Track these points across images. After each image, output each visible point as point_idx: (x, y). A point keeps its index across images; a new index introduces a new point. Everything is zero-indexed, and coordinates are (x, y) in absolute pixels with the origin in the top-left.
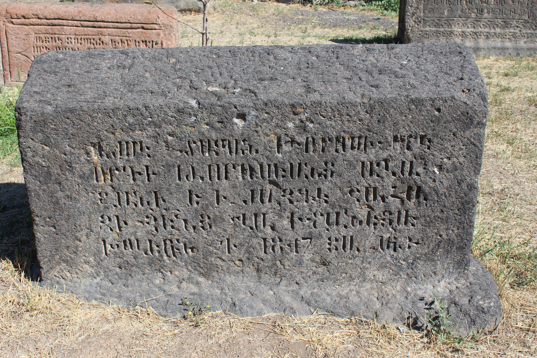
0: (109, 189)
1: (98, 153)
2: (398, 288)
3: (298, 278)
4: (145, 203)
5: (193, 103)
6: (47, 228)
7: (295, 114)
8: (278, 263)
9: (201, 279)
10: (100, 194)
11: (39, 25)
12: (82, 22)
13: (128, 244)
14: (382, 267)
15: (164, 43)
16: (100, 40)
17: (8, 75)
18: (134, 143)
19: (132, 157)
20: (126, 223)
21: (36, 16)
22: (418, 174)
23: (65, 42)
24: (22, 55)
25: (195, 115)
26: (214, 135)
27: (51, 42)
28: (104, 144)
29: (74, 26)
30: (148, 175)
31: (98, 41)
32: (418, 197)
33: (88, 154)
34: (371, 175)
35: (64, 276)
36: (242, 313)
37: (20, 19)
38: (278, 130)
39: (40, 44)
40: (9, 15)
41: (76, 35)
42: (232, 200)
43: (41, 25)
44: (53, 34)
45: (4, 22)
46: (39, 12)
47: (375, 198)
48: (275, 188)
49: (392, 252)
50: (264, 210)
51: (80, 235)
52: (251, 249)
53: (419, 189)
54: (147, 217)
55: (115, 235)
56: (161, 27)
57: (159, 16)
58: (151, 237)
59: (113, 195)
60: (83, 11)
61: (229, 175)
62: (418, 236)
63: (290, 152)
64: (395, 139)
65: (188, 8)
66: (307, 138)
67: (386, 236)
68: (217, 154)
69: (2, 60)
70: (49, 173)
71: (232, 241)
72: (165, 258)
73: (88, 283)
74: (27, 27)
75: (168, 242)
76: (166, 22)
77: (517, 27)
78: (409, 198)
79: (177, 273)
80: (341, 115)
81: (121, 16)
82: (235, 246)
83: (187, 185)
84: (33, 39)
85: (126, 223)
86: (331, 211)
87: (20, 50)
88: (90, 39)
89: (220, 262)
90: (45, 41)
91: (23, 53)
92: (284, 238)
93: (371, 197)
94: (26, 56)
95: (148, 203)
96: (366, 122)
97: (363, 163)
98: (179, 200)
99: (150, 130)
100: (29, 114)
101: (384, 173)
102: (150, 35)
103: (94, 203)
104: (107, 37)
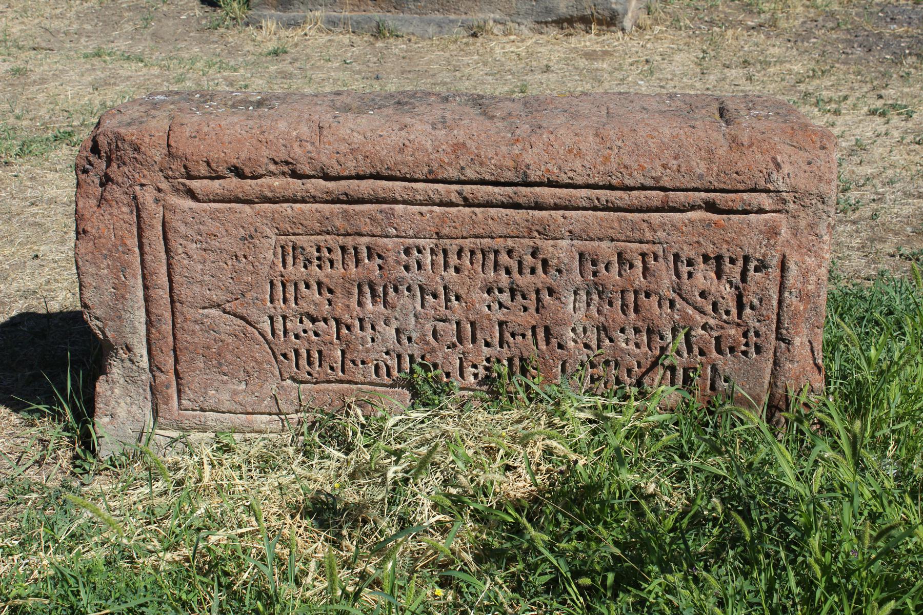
11: (295, 201)
12: (467, 188)
15: (793, 268)
16: (534, 255)
17: (168, 387)
21: (285, 168)
23: (398, 263)
24: (225, 312)
27: (339, 265)
29: (434, 204)
31: (529, 260)
37: (224, 178)
39: (295, 271)
40: (177, 165)
41: (439, 236)
43: (303, 201)
44: (349, 234)
45: (159, 190)
46: (297, 151)
56: (785, 202)
57: (779, 158)
60: (469, 143)
65: (580, 14)
69: (148, 330)
74: (246, 208)
76: (802, 183)
81: (627, 160)
84: (270, 256)
87: (217, 296)
88: (496, 252)
90: (316, 262)
94: (242, 318)
102: (740, 232)
104: (564, 243)
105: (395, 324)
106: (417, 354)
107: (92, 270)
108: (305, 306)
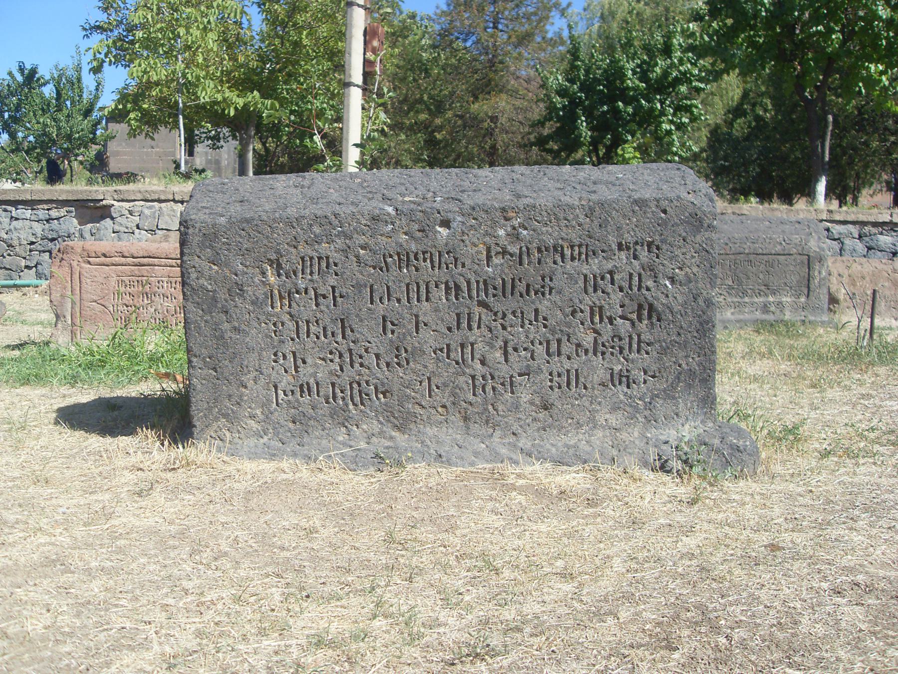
0: (286, 318)
1: (275, 272)
2: (636, 434)
3: (515, 427)
4: (329, 333)
5: (390, 210)
6: (205, 371)
7: (506, 219)
8: (490, 407)
9: (393, 434)
10: (274, 325)
13: (305, 390)
14: (615, 409)
18: (320, 258)
19: (316, 277)
20: (304, 362)
22: (648, 289)
25: (393, 223)
26: (413, 247)
27: (136, 287)
28: (283, 261)
30: (334, 298)
32: (650, 317)
33: (263, 273)
34: (595, 291)
35: (222, 437)
36: (449, 463)
38: (487, 239)
39: (122, 289)
40: (85, 253)
41: (169, 277)
42: (434, 327)
46: (124, 249)
47: (601, 320)
48: (485, 310)
49: (625, 389)
50: (472, 339)
51: (248, 379)
52: (458, 391)
53: (651, 306)
54: (331, 353)
55: (290, 378)
58: (334, 379)
59: (291, 325)
61: (430, 295)
62: (654, 367)
63: (502, 265)
64: (620, 247)
66: (521, 248)
67: (617, 368)
68: (417, 270)
70: (215, 300)
71: (434, 381)
72: (351, 407)
73: (252, 444)
74: (107, 267)
75: (355, 386)
77: (721, 294)
78: (640, 319)
79: (365, 427)
80: (558, 219)
82: (438, 388)
83: (381, 309)
84: (113, 283)
85: (304, 362)
86: (551, 337)
87: (95, 298)
89: (418, 410)
91: (99, 302)
92: (496, 374)
93: (597, 319)
95: (333, 334)
96: (586, 227)
97: (585, 276)
98: (370, 329)
99: (340, 243)
100: (197, 225)
101: (609, 287)
103: (267, 336)
105: (154, 307)
106: (161, 318)
107: (55, 288)
108: (125, 301)
